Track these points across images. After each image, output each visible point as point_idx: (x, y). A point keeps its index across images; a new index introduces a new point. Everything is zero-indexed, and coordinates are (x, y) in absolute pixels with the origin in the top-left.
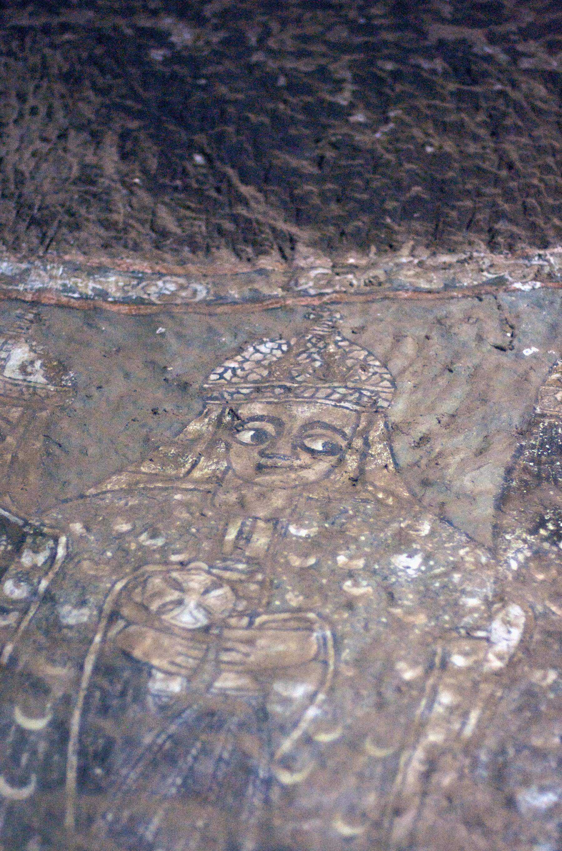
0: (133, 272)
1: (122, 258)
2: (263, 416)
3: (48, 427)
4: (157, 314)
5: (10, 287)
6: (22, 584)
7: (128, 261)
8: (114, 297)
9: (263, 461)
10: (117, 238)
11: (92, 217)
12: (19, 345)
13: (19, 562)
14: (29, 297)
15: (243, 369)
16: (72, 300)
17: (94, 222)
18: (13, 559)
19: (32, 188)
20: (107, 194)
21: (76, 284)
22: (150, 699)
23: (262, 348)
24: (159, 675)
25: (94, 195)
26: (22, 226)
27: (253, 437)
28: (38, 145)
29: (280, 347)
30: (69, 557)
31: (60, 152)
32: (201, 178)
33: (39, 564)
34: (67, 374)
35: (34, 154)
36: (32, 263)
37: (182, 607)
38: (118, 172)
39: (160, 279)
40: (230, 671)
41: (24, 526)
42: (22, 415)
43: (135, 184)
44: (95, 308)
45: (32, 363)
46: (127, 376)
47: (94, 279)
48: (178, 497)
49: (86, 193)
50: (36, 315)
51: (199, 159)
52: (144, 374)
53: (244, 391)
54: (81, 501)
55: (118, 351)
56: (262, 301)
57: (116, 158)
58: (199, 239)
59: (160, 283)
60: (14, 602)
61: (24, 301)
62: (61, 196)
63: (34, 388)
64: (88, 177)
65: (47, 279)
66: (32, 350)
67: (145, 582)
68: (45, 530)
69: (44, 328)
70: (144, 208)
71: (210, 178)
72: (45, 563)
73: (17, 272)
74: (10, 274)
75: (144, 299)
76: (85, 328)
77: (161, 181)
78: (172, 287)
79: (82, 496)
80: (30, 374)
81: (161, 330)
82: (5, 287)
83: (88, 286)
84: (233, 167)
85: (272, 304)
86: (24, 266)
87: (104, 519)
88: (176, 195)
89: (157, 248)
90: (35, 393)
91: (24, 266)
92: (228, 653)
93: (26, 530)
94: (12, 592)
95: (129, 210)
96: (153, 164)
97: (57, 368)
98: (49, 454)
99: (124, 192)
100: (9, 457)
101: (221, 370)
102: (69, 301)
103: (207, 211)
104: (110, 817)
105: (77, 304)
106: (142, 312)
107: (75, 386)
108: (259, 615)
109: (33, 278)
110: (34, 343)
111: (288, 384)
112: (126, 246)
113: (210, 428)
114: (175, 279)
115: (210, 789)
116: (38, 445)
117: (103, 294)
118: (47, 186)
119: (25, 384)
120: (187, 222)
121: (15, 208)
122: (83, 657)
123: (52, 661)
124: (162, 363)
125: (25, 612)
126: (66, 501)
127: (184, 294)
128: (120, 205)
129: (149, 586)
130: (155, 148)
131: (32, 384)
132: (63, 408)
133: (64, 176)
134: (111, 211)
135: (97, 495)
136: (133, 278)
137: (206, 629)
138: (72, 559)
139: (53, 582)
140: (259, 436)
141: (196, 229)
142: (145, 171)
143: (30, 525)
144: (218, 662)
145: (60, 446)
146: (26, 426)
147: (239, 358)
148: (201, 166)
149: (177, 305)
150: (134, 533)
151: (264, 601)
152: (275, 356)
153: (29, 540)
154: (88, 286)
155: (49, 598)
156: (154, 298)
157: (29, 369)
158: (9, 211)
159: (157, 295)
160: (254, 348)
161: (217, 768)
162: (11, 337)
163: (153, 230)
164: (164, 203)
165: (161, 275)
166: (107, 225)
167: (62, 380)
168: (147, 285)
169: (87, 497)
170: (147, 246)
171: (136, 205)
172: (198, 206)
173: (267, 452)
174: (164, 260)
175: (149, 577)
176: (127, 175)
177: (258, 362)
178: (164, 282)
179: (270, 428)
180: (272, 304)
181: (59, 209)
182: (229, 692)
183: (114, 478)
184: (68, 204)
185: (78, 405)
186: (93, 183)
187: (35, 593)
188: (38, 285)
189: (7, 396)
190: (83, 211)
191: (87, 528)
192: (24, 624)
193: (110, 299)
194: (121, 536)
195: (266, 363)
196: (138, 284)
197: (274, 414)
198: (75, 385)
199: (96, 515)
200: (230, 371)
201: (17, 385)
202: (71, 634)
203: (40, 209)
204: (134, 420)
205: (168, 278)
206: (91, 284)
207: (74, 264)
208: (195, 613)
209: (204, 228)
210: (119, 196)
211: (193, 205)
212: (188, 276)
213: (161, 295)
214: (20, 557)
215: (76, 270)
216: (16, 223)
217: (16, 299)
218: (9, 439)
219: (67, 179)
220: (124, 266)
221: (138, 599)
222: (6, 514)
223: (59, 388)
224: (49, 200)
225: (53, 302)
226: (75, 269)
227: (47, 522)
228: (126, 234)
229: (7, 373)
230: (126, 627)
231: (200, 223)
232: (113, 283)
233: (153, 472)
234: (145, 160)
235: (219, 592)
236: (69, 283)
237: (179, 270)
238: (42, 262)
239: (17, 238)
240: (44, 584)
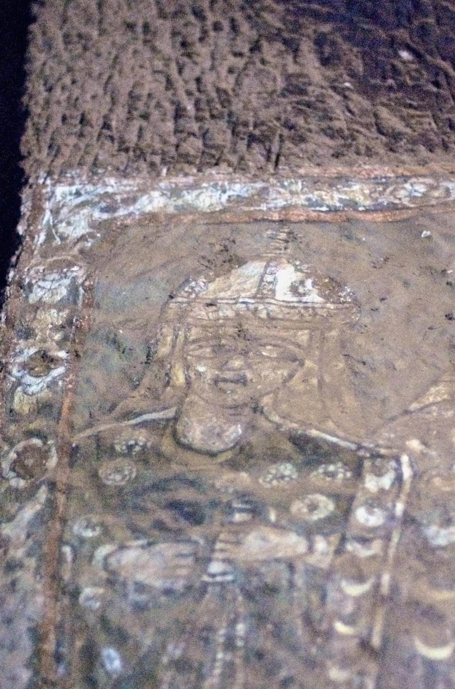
0: (376, 178)
1: (360, 166)
3: (343, 347)
4: (415, 218)
5: (252, 209)
6: (376, 510)
7: (367, 167)
8: (364, 206)
10: (345, 146)
11: (312, 127)
12: (283, 266)
13: (364, 488)
14: (276, 217)
16: (322, 214)
17: (317, 133)
18: (355, 486)
19: (241, 105)
20: (323, 102)
21: (321, 196)
25: (309, 105)
26: (242, 146)
28: (232, 60)
30: (416, 476)
31: (259, 65)
32: (413, 74)
34: (344, 290)
35: (231, 71)
36: (267, 181)
38: (326, 78)
39: (406, 182)
42: (311, 338)
43: (348, 89)
44: (348, 220)
45: (302, 283)
46: (406, 284)
47: (338, 190)
49: (298, 103)
50: (289, 233)
51: (405, 55)
52: (424, 281)
54: (407, 418)
55: (386, 260)
57: (317, 64)
58: (432, 136)
59: (407, 186)
60: (373, 530)
61: (274, 221)
62: (273, 111)
63: (313, 308)
64: (295, 87)
65: (288, 196)
66: (297, 270)
68: (383, 451)
69: (301, 246)
70: (364, 112)
71: (424, 72)
72: (393, 484)
73: (254, 192)
74: (246, 195)
75: (397, 204)
76: (344, 241)
77: (373, 81)
78: (422, 189)
79: (406, 412)
80: (304, 294)
81: (425, 233)
82: (246, 209)
83: (334, 198)
84: (444, 59)
86: (259, 185)
87: (438, 432)
88: (392, 95)
89: (391, 150)
90: (316, 314)
91: (259, 185)
93: (361, 453)
94: (367, 520)
95: (349, 114)
96: (359, 66)
97: (331, 286)
98: (356, 373)
99: (338, 98)
100: (315, 381)
102: (319, 216)
103: (431, 107)
105: (328, 217)
107: (355, 301)
109: (274, 196)
110: (298, 263)
112: (358, 153)
114: (421, 180)
116: (341, 365)
117: (353, 205)
118: (255, 102)
119: (302, 305)
120: (413, 121)
121: (228, 128)
123: (435, 585)
124: (440, 267)
125: (388, 538)
126: (393, 419)
127: (436, 194)
128: (338, 111)
130: (355, 49)
131: (310, 305)
132: (352, 326)
133: (270, 90)
134: (331, 119)
135: (421, 409)
136: (378, 184)
138: (421, 477)
139: (408, 504)
141: (427, 127)
142: (353, 75)
143: (366, 449)
145: (364, 363)
146: (321, 348)
148: (409, 62)
149: (433, 206)
153: (367, 464)
154: (334, 198)
155: (409, 520)
156: (406, 202)
157: (301, 290)
158: (224, 132)
159: (408, 199)
162: (271, 259)
163: (383, 134)
164: (383, 104)
165: (406, 179)
166: (332, 133)
167: (340, 296)
168: (395, 190)
169: (411, 412)
170: (382, 151)
171: (355, 110)
172: (421, 103)
174: (403, 162)
176: (335, 80)
178: (412, 185)
181: (275, 122)
183: (433, 390)
184: (283, 116)
185: (366, 320)
186: (303, 92)
187: (392, 517)
188: (281, 203)
189: (287, 320)
190: (301, 121)
191: (425, 443)
192: (392, 552)
193: (361, 209)
196: (385, 190)
198: (355, 301)
199: (428, 430)
201: (294, 307)
202: (446, 555)
203: (256, 126)
204: (431, 328)
205: (414, 180)
206: (337, 196)
207: (313, 177)
209: (434, 125)
210: (334, 101)
211: (415, 104)
212: (434, 175)
213: (413, 199)
214: (364, 483)
215: (315, 183)
216: (234, 144)
217: (264, 220)
218: (308, 363)
219: (274, 91)
220: (364, 173)
222: (334, 440)
223: (340, 306)
224: (263, 115)
225: (302, 218)
226: (315, 182)
227: (381, 442)
228: (354, 140)
229: (279, 296)
231: (427, 120)
232: (359, 192)
234: (349, 63)
236: (314, 196)
237: (422, 170)
238: (277, 178)
239: (242, 158)
240: (400, 508)
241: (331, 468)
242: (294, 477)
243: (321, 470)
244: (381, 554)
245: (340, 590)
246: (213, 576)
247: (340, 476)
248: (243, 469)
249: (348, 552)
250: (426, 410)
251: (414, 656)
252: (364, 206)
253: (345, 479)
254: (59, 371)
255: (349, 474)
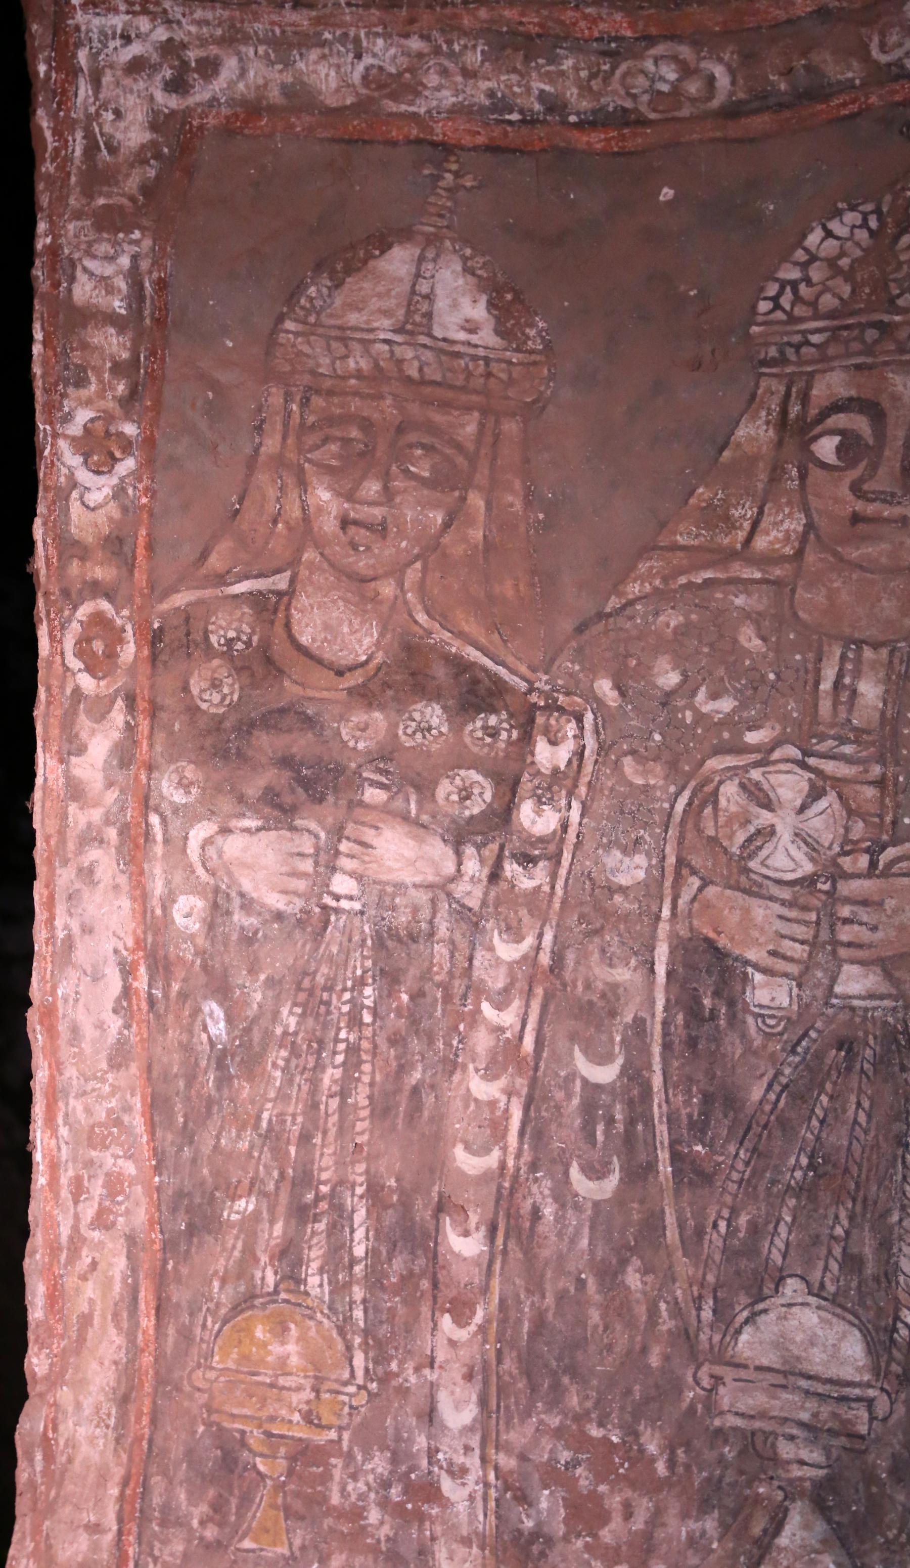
2: (851, 399)
6: (545, 807)
9: (859, 506)
15: (808, 281)
22: (750, 1020)
23: (834, 225)
24: (758, 977)
27: (839, 449)
29: (865, 224)
33: (562, 768)
37: (775, 840)
40: (852, 962)
41: (531, 690)
42: (482, 426)
48: (739, 601)
53: (815, 339)
56: (826, 98)
67: (716, 793)
72: (570, 762)
79: (601, 616)
85: (844, 105)
92: (847, 927)
93: (534, 698)
101: (772, 289)
104: (723, 1225)
106: (630, 145)
108: (883, 848)
111: (886, 318)
113: (771, 433)
115: (846, 1170)
122: (652, 949)
129: (723, 802)
135: (624, 607)
137: (809, 882)
140: (850, 447)
144: (835, 943)
147: (800, 255)
150: (687, 688)
151: (888, 819)
152: (858, 244)
153: (540, 720)
160: (824, 228)
161: (852, 1137)
173: (865, 487)
175: (721, 782)
177: (832, 263)
179: (861, 424)
180: (844, 105)
182: (856, 1003)
194: (667, 698)
195: (844, 262)
197: (867, 394)
200: (788, 289)
208: (794, 852)
221: (711, 832)
230: (700, 889)
233: (696, 542)
235: (823, 804)
241: (493, 720)
242: (444, 729)
243: (479, 724)
244: (546, 889)
245: (491, 949)
246: (337, 898)
247: (504, 735)
248: (382, 707)
249: (506, 880)
250: (629, 611)
251: (573, 1075)
252: (578, 114)
253: (509, 743)
254: (128, 465)
255: (515, 734)
